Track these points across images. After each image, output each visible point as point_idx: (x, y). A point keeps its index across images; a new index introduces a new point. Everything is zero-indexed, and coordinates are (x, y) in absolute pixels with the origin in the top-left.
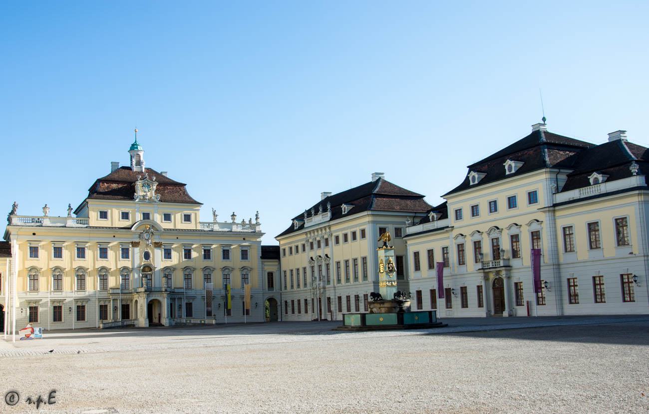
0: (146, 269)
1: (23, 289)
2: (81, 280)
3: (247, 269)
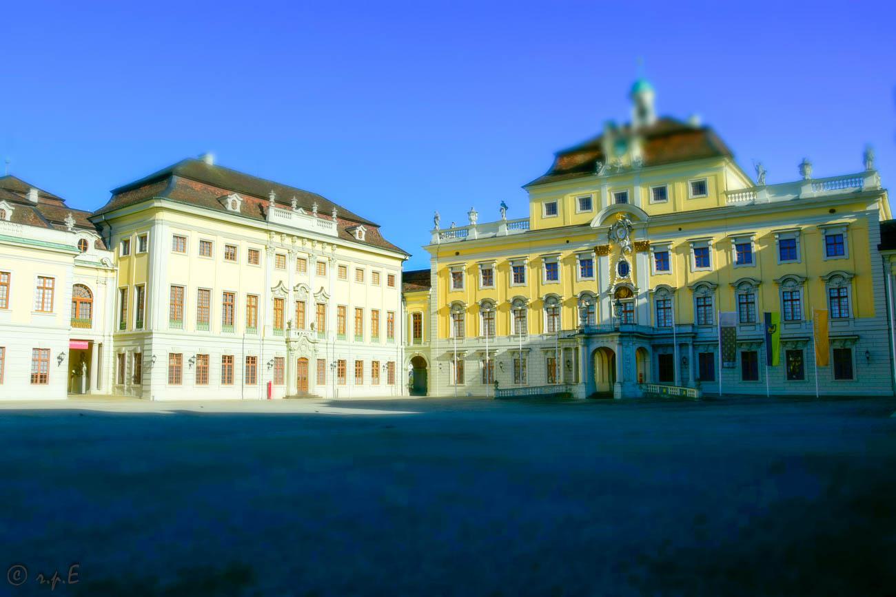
0: (623, 293)
1: (507, 334)
2: (489, 319)
3: (795, 281)
